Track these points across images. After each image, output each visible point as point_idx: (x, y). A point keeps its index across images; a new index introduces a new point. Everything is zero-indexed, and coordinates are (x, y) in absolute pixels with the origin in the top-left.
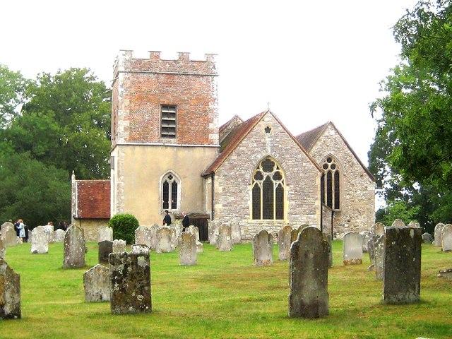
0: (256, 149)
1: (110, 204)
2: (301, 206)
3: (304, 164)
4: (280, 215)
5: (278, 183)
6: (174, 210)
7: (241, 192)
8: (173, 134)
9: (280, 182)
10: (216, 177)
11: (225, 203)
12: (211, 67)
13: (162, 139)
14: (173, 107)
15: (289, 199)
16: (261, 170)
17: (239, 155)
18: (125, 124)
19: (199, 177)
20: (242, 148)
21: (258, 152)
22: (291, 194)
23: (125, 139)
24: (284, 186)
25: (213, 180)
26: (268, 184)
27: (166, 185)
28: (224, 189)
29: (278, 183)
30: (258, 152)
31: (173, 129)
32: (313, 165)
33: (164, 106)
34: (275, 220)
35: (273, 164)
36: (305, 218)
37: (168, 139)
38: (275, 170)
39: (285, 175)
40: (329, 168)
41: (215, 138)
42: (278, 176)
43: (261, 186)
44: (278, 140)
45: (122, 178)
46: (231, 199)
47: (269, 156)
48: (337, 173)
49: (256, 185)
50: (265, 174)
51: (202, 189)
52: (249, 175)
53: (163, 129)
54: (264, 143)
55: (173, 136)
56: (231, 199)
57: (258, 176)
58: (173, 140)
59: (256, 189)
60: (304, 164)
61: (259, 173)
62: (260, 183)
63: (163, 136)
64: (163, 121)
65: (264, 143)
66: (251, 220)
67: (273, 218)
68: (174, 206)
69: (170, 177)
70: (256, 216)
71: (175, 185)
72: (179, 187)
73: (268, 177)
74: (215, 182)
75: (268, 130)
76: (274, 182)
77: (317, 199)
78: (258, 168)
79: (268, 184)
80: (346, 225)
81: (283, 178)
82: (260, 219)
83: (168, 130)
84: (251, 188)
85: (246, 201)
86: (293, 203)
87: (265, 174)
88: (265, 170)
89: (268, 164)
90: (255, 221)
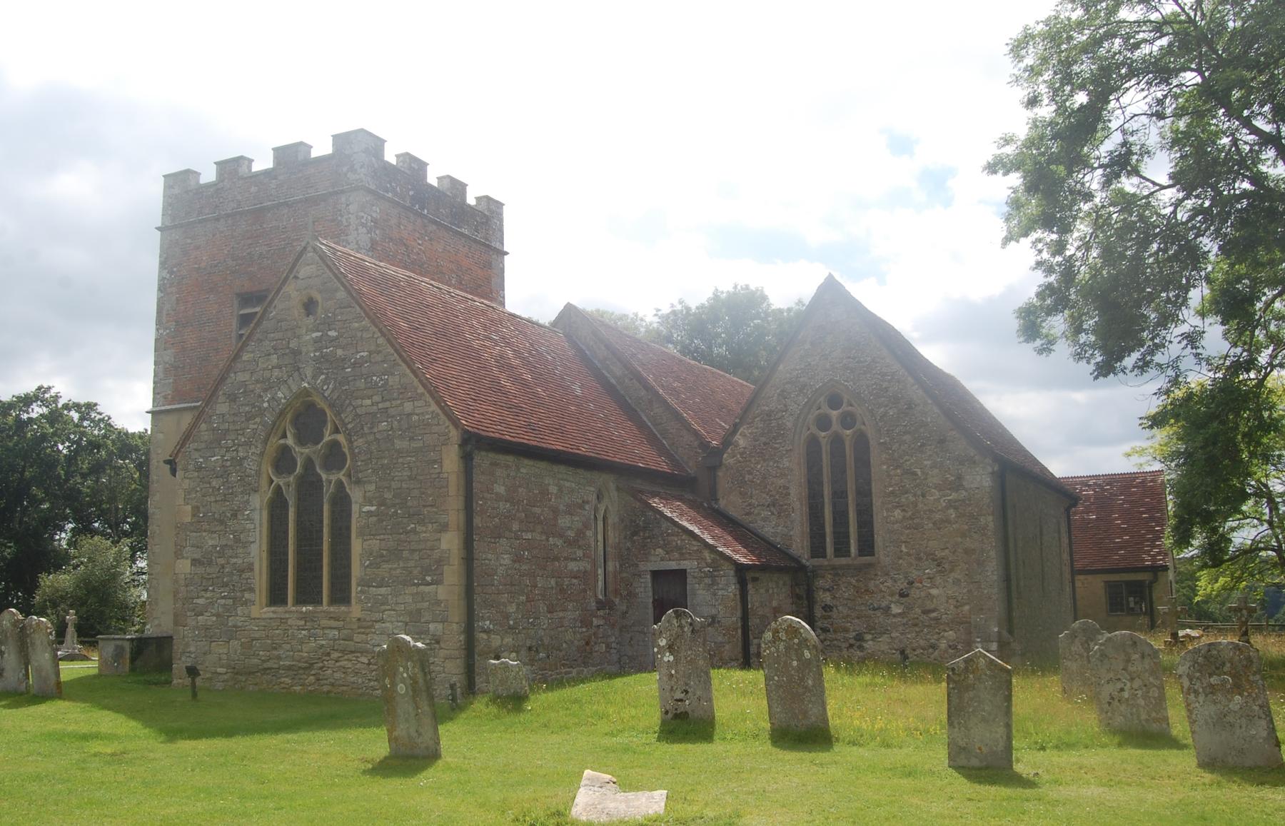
0: (276, 373)
1: (349, 566)
3: (408, 407)
4: (341, 594)
5: (334, 478)
7: (235, 516)
9: (341, 475)
11: (196, 556)
12: (345, 169)
15: (361, 534)
16: (290, 441)
17: (232, 398)
18: (167, 359)
20: (242, 377)
21: (281, 382)
22: (370, 513)
23: (165, 397)
26: (309, 487)
28: (196, 510)
29: (334, 478)
30: (281, 382)
32: (434, 407)
34: (325, 607)
36: (409, 599)
38: (327, 438)
39: (351, 449)
40: (836, 427)
42: (334, 457)
44: (333, 333)
47: (306, 393)
48: (862, 442)
49: (279, 487)
57: (283, 461)
59: (277, 506)
60: (408, 407)
61: (285, 452)
62: (288, 483)
65: (296, 353)
66: (260, 610)
67: (321, 603)
70: (276, 596)
73: (309, 464)
75: (309, 306)
76: (324, 477)
77: (444, 528)
78: (284, 436)
79: (309, 487)
80: (896, 610)
82: (283, 601)
85: (246, 545)
86: (375, 544)
87: (301, 453)
88: (301, 441)
89: (307, 419)
90: (269, 612)
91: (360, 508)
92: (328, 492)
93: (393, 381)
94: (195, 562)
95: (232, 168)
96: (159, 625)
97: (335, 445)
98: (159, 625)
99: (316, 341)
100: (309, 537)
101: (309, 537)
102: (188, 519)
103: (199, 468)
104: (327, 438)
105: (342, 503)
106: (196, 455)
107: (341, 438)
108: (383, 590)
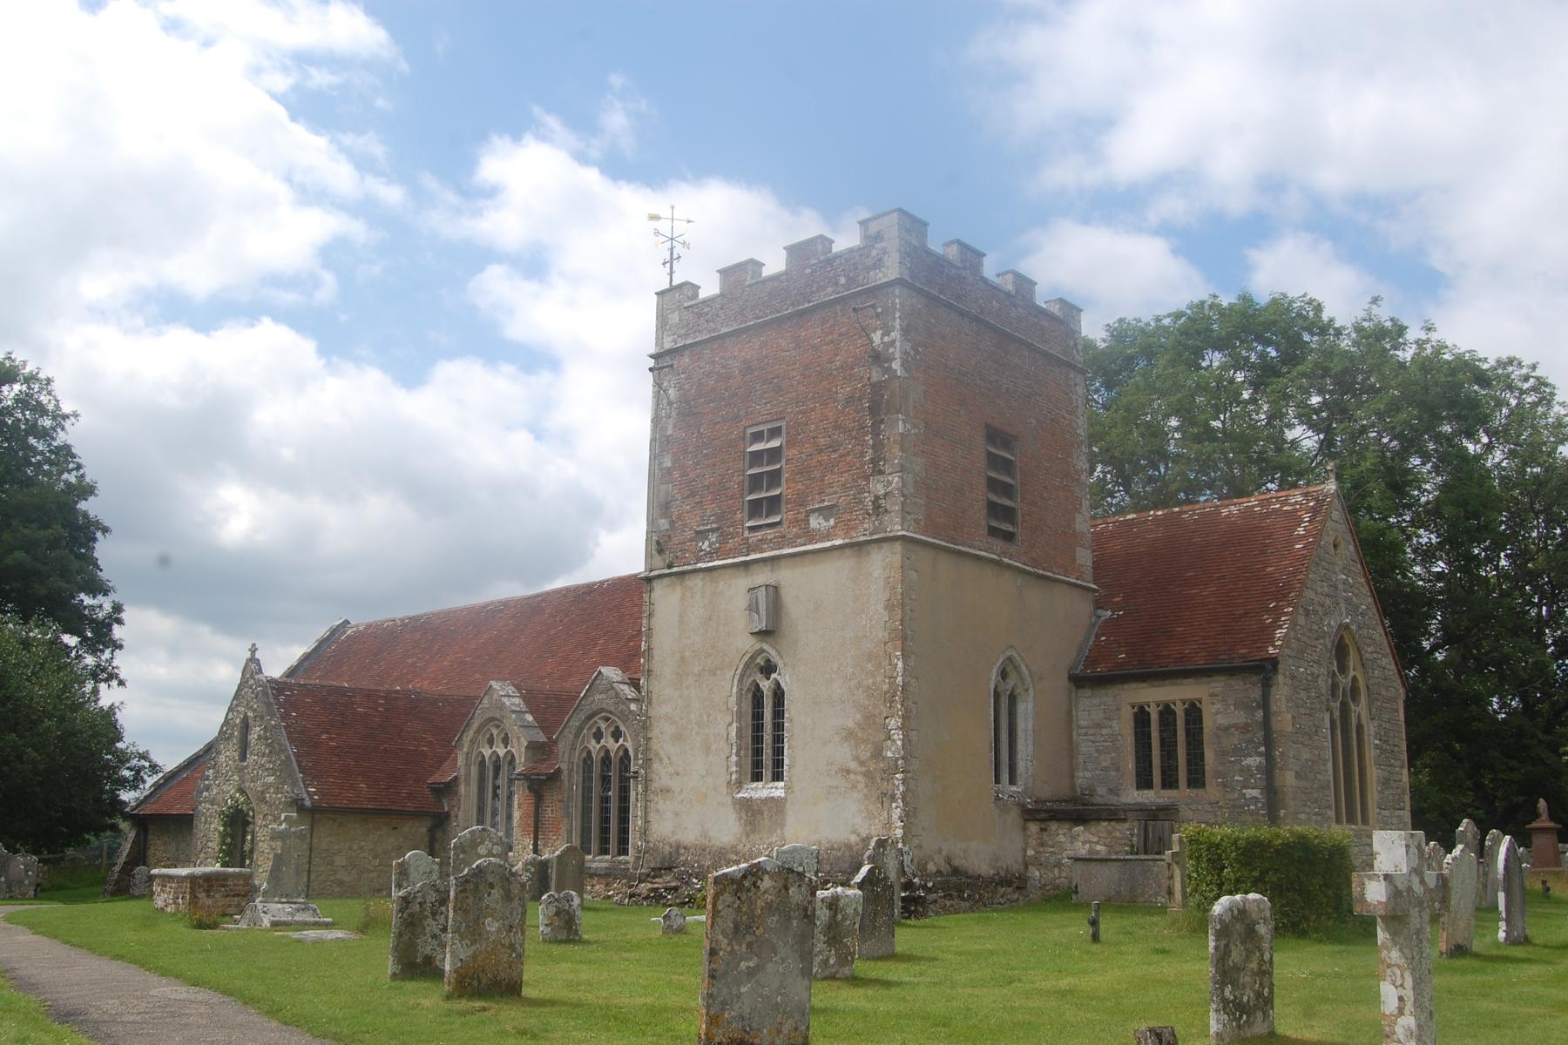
6: (1014, 788)
8: (1011, 529)
10: (1280, 678)
13: (990, 540)
17: (1307, 614)
19: (1063, 681)
23: (917, 521)
24: (1364, 715)
25: (1267, 685)
33: (994, 436)
37: (998, 544)
38: (1352, 673)
41: (1085, 557)
42: (1355, 691)
43: (1337, 714)
45: (912, 662)
52: (1324, 684)
53: (994, 510)
54: (1336, 588)
55: (1009, 537)
56: (1305, 755)
58: (1013, 549)
62: (1336, 705)
63: (993, 532)
68: (1012, 781)
71: (1013, 699)
72: (1025, 708)
81: (1363, 698)
83: (1002, 519)
91: (1371, 740)
92: (1354, 722)
93: (1377, 637)
94: (1298, 775)
96: (920, 847)
97: (1354, 679)
98: (920, 847)
99: (1345, 582)
102: (1290, 729)
103: (1293, 677)
105: (1360, 727)
106: (1290, 661)
108: (1386, 813)
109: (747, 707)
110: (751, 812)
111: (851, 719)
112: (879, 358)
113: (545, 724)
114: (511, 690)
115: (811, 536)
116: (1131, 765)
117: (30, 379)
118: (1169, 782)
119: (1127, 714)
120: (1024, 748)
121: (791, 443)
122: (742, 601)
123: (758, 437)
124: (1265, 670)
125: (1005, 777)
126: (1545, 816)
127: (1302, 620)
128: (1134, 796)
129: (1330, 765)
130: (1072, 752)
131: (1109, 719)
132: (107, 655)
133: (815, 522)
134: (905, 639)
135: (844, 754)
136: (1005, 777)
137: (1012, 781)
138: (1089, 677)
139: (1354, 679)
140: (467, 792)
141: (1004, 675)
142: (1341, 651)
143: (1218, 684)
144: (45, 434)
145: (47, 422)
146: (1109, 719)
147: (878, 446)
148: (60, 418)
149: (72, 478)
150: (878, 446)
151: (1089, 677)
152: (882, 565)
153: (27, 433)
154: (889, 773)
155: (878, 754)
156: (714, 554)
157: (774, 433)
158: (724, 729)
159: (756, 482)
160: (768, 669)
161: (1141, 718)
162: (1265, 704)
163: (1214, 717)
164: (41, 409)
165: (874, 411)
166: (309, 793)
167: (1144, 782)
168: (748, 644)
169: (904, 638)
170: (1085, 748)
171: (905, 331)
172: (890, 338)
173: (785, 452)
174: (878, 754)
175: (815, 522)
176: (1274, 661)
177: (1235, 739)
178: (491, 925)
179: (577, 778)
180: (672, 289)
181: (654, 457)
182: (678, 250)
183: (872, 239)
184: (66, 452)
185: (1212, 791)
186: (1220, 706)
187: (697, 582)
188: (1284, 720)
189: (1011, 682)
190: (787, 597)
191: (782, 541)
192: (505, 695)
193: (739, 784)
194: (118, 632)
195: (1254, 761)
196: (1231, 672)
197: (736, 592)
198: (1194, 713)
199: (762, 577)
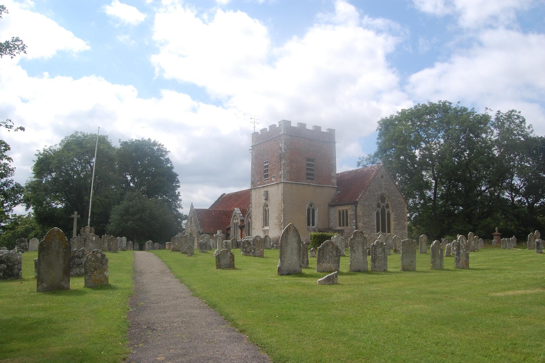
2: (398, 224)
4: (389, 231)
10: (358, 205)
14: (312, 160)
17: (369, 192)
24: (391, 212)
25: (356, 207)
27: (309, 210)
28: (363, 213)
31: (313, 175)
33: (308, 160)
35: (385, 199)
37: (309, 181)
38: (386, 202)
42: (387, 206)
43: (380, 211)
46: (366, 220)
50: (382, 204)
51: (328, 213)
52: (374, 205)
55: (313, 179)
56: (366, 220)
57: (379, 206)
58: (313, 181)
59: (378, 214)
61: (379, 203)
63: (307, 178)
64: (308, 169)
68: (313, 225)
69: (311, 206)
72: (316, 212)
74: (358, 208)
75: (382, 177)
81: (390, 208)
84: (375, 213)
85: (374, 221)
87: (382, 204)
89: (383, 199)
92: (386, 212)
95: (302, 126)
97: (387, 204)
100: (383, 221)
101: (383, 221)
103: (363, 205)
104: (386, 202)
105: (389, 214)
107: (389, 203)
109: (265, 213)
110: (265, 231)
111: (277, 215)
112: (281, 149)
113: (244, 216)
114: (239, 209)
115: (272, 182)
116: (338, 222)
117: (160, 145)
118: (343, 226)
119: (338, 212)
120: (316, 219)
121: (270, 164)
122: (263, 193)
123: (265, 163)
124: (356, 204)
125: (311, 225)
126: (497, 231)
127: (367, 193)
128: (339, 228)
129: (375, 222)
130: (329, 220)
131: (335, 213)
132: (179, 202)
133: (273, 179)
134: (284, 201)
135: (276, 221)
136: (311, 225)
137: (313, 225)
138: (332, 205)
139: (387, 204)
140: (232, 229)
141: (311, 206)
142: (383, 199)
143: (350, 206)
144: (163, 156)
145: (164, 153)
146: (335, 213)
147: (280, 165)
148: (166, 152)
149: (169, 165)
150: (280, 165)
151: (332, 205)
152: (281, 186)
153: (160, 156)
154: (281, 225)
155: (280, 221)
156: (260, 185)
157: (268, 162)
158: (261, 217)
159: (265, 171)
160: (267, 206)
161: (340, 212)
162: (356, 211)
163: (350, 212)
164: (162, 151)
165: (280, 159)
166: (201, 230)
167: (340, 226)
168: (264, 201)
169: (284, 200)
170: (332, 219)
171: (285, 144)
172: (282, 145)
173: (269, 166)
174: (280, 221)
175: (273, 179)
176: (357, 202)
177: (352, 217)
178: (176, 243)
179: (247, 226)
180: (255, 133)
181: (252, 166)
182: (256, 125)
183: (280, 125)
184: (168, 160)
185: (349, 227)
186: (350, 210)
187: (257, 190)
188: (360, 213)
189: (312, 207)
190: (269, 192)
191: (269, 183)
192: (237, 210)
193: (263, 227)
194: (179, 197)
195: (354, 221)
196: (352, 204)
197: (262, 191)
198: (347, 211)
199: (266, 189)
